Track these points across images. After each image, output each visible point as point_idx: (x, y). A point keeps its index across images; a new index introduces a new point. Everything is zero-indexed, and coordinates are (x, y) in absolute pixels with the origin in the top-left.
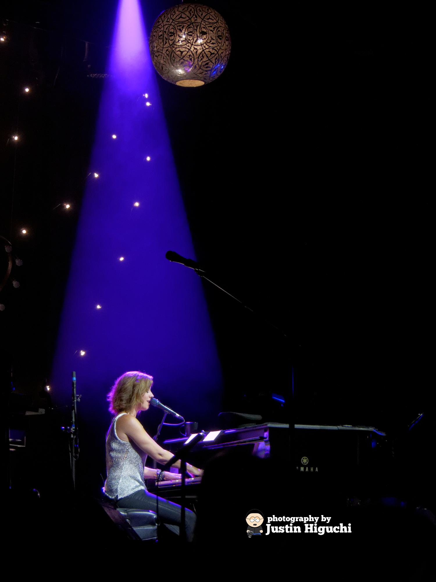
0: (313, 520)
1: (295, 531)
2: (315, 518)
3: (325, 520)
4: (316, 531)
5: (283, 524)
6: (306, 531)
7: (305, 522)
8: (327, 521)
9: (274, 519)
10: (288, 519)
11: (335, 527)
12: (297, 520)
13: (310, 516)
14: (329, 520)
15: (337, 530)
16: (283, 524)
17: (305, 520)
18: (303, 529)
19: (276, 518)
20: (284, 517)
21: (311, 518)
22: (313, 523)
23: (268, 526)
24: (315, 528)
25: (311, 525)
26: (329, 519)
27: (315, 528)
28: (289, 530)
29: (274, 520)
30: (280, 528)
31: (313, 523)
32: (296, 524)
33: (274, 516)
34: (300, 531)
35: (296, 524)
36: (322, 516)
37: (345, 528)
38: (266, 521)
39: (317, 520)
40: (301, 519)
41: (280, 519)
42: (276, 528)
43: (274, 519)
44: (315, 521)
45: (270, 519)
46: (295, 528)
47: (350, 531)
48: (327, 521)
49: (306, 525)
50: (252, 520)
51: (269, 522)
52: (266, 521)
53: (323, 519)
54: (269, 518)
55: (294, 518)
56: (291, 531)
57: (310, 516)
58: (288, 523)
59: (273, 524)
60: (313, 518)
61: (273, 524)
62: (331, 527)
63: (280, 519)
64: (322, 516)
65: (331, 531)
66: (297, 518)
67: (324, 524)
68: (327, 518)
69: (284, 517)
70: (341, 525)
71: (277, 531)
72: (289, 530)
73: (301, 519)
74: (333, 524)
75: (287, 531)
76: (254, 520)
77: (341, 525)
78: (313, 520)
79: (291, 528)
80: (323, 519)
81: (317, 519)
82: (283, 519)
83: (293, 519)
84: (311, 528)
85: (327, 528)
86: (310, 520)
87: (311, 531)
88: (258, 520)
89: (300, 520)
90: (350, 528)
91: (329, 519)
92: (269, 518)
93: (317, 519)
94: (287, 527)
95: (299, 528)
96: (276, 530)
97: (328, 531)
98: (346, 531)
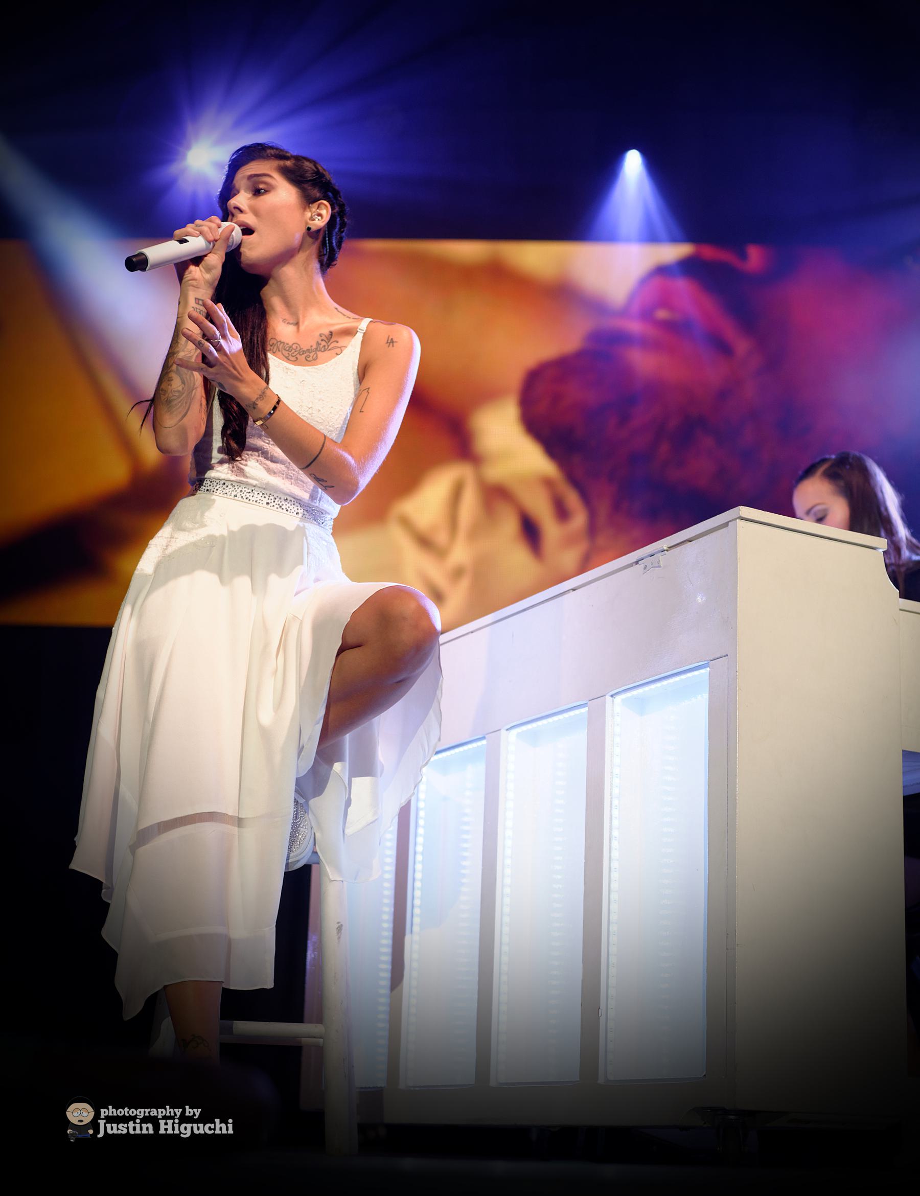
0: (173, 1114)
2: (176, 1110)
3: (191, 1114)
7: (160, 1117)
8: (194, 1115)
10: (133, 1112)
12: (147, 1114)
13: (168, 1107)
14: (197, 1114)
16: (125, 1120)
17: (161, 1113)
19: (114, 1110)
20: (126, 1109)
21: (169, 1111)
22: (172, 1118)
26: (197, 1112)
29: (111, 1114)
31: (172, 1118)
32: (145, 1120)
33: (110, 1107)
35: (145, 1120)
36: (187, 1107)
38: (97, 1116)
39: (178, 1114)
40: (154, 1112)
41: (121, 1112)
43: (111, 1111)
44: (176, 1115)
45: (104, 1113)
48: (194, 1115)
50: (76, 1114)
51: (102, 1116)
52: (97, 1116)
53: (189, 1112)
54: (102, 1111)
55: (142, 1110)
57: (168, 1107)
58: (134, 1119)
59: (109, 1119)
60: (172, 1110)
61: (109, 1119)
63: (121, 1112)
64: (187, 1107)
66: (147, 1111)
67: (190, 1120)
68: (195, 1110)
69: (126, 1109)
73: (154, 1112)
74: (203, 1119)
76: (79, 1113)
78: (173, 1114)
80: (189, 1112)
81: (178, 1112)
82: (126, 1112)
83: (141, 1113)
86: (168, 1114)
88: (85, 1114)
89: (152, 1114)
91: (197, 1112)
92: (102, 1111)
93: (178, 1112)
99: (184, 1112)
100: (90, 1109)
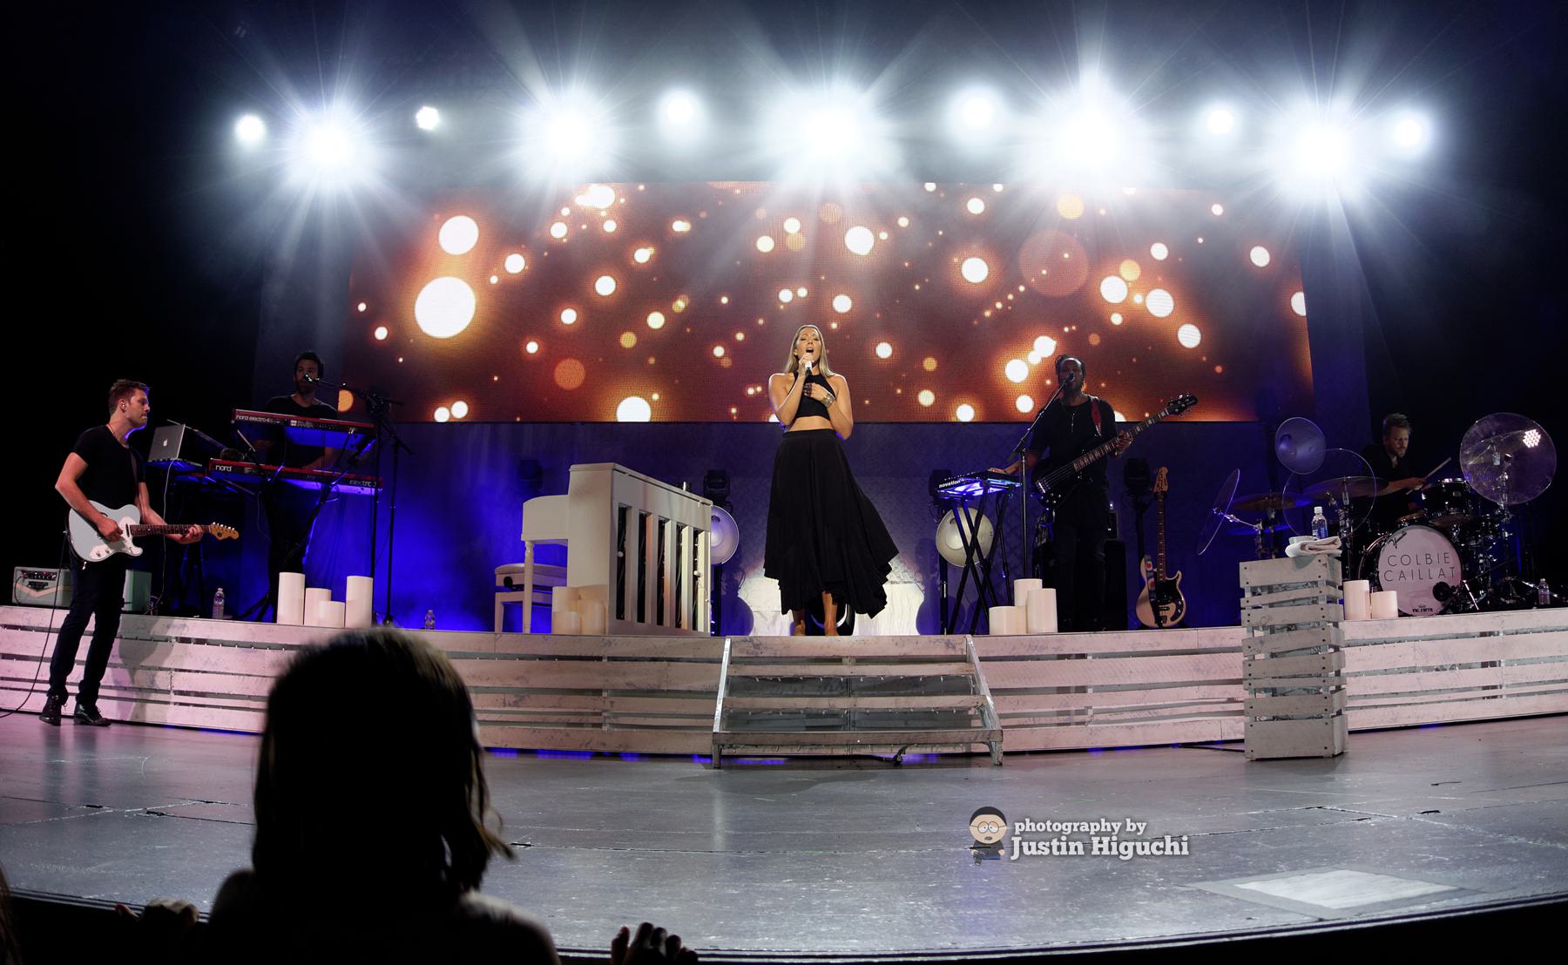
1: (1072, 852)
4: (1114, 852)
5: (1047, 836)
6: (1095, 852)
9: (1029, 826)
11: (1155, 844)
15: (1158, 848)
16: (1047, 836)
18: (1088, 847)
21: (1105, 826)
23: (1016, 840)
24: (1114, 845)
25: (1106, 840)
27: (1114, 845)
28: (1059, 848)
30: (1040, 845)
34: (1081, 852)
37: (1176, 845)
41: (1041, 827)
42: (1033, 844)
43: (1029, 826)
46: (1072, 845)
47: (1185, 852)
49: (1095, 840)
50: (982, 829)
56: (1064, 852)
62: (1146, 844)
63: (1041, 827)
65: (1147, 852)
70: (1168, 839)
71: (1034, 852)
72: (1059, 848)
73: (1085, 827)
75: (1055, 852)
77: (1168, 839)
79: (1063, 845)
83: (1067, 828)
84: (1105, 846)
85: (1139, 845)
87: (1105, 852)
88: (994, 829)
90: (1185, 845)
94: (1055, 843)
95: (1080, 847)
96: (1031, 849)
97: (1139, 852)
98: (1177, 852)
99: (1125, 825)
100: (1001, 822)
